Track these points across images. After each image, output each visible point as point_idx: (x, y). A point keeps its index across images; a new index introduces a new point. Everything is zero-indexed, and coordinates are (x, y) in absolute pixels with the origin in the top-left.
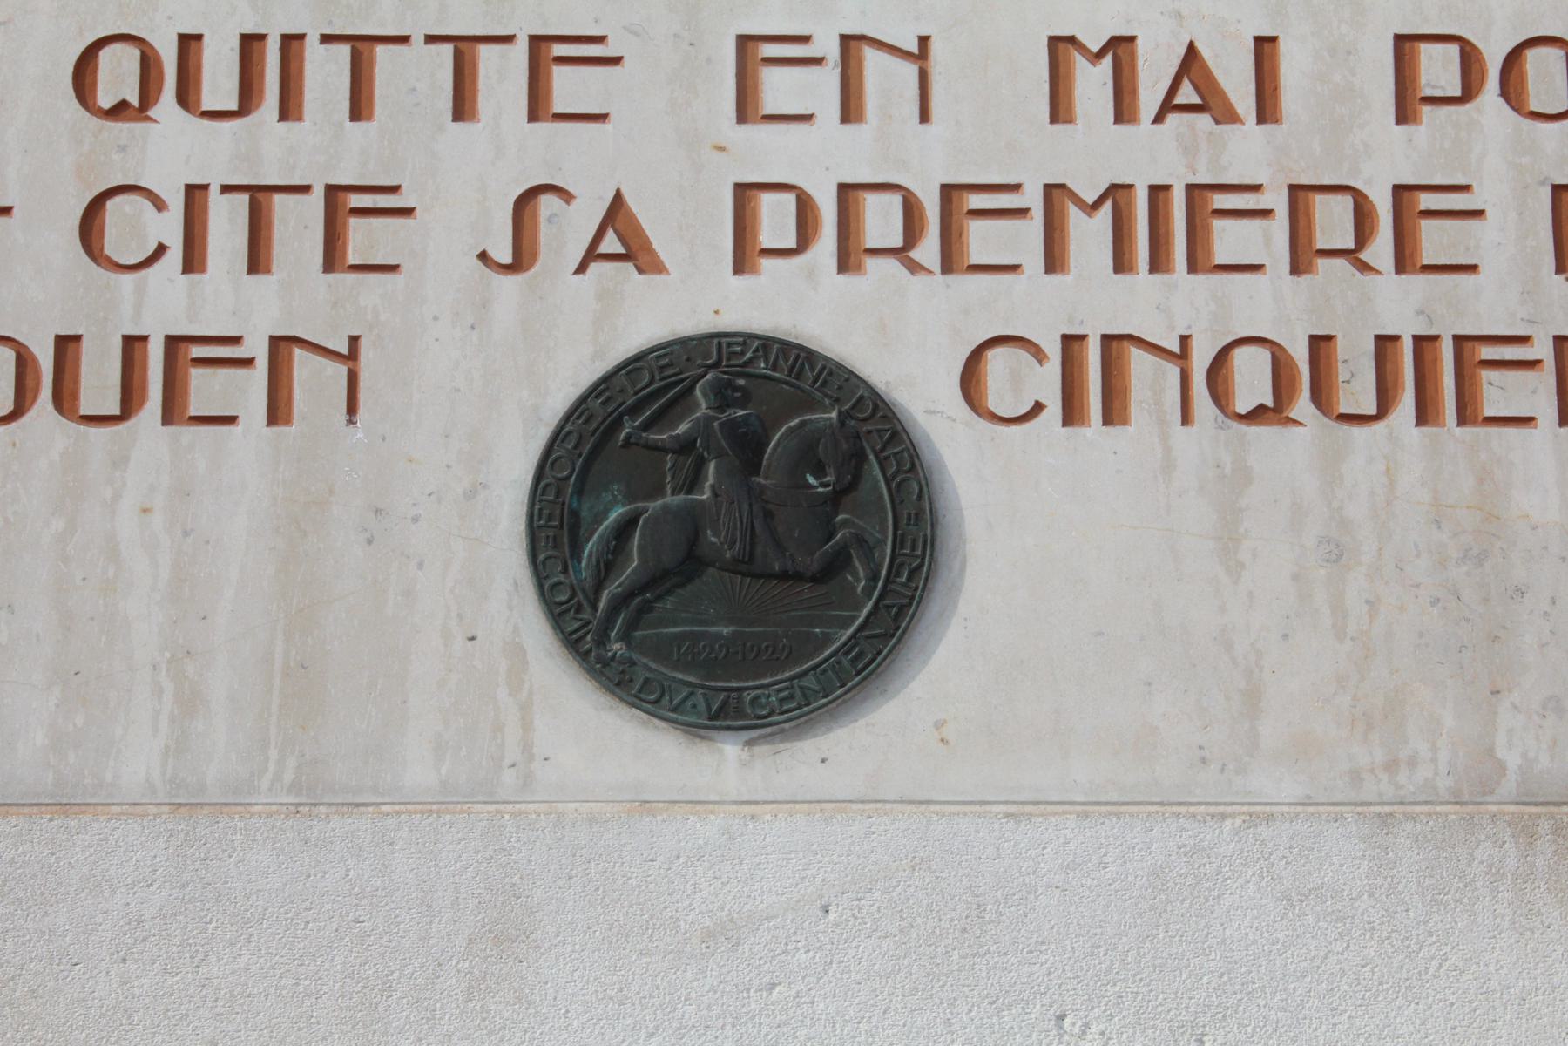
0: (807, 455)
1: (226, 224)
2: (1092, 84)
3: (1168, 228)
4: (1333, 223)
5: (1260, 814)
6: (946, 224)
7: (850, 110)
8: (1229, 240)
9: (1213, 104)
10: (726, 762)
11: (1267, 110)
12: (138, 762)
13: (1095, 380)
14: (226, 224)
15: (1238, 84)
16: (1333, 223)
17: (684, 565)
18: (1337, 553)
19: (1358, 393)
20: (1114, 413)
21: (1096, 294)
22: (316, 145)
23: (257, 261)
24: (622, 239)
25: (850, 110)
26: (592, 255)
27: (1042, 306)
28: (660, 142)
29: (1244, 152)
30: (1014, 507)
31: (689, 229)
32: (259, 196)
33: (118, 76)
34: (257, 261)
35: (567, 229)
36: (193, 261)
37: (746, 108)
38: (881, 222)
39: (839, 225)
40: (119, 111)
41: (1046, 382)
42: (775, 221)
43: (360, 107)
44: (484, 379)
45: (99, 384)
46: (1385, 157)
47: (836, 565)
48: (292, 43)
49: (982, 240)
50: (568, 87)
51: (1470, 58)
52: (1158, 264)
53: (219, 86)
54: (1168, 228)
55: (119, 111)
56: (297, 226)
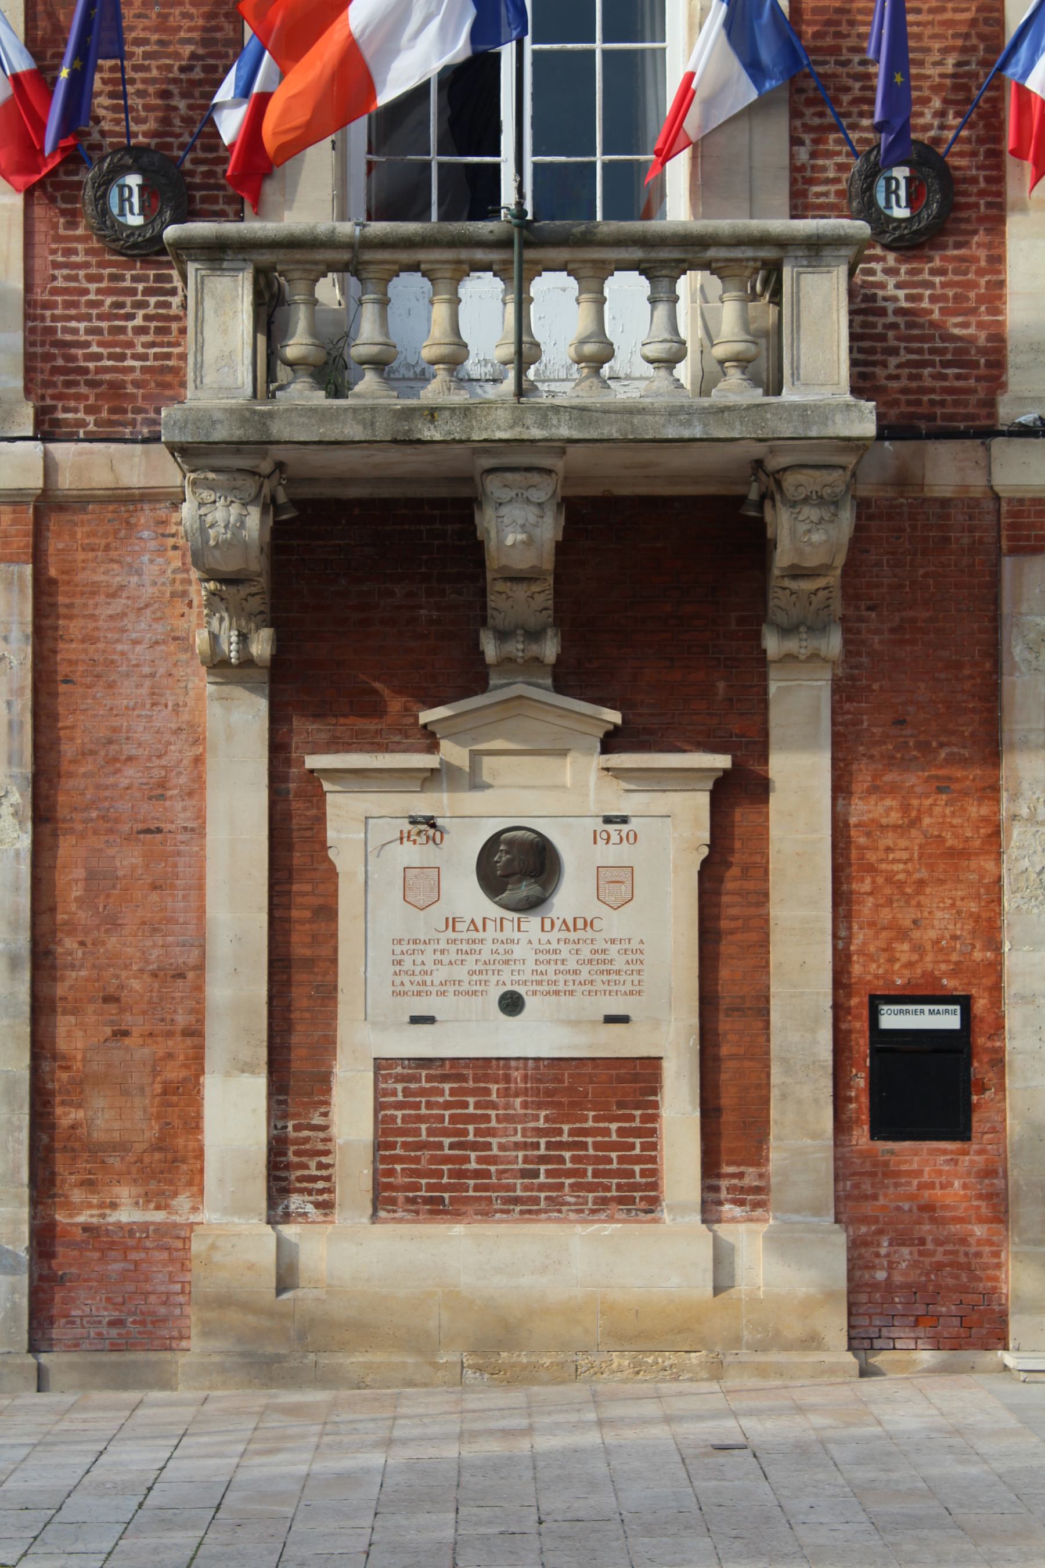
3: (540, 983)
6: (525, 982)
13: (534, 993)
21: (535, 987)
22: (483, 977)
24: (504, 984)
27: (531, 988)
28: (506, 976)
29: (545, 978)
30: (529, 1001)
31: (508, 983)
46: (554, 978)
54: (540, 983)
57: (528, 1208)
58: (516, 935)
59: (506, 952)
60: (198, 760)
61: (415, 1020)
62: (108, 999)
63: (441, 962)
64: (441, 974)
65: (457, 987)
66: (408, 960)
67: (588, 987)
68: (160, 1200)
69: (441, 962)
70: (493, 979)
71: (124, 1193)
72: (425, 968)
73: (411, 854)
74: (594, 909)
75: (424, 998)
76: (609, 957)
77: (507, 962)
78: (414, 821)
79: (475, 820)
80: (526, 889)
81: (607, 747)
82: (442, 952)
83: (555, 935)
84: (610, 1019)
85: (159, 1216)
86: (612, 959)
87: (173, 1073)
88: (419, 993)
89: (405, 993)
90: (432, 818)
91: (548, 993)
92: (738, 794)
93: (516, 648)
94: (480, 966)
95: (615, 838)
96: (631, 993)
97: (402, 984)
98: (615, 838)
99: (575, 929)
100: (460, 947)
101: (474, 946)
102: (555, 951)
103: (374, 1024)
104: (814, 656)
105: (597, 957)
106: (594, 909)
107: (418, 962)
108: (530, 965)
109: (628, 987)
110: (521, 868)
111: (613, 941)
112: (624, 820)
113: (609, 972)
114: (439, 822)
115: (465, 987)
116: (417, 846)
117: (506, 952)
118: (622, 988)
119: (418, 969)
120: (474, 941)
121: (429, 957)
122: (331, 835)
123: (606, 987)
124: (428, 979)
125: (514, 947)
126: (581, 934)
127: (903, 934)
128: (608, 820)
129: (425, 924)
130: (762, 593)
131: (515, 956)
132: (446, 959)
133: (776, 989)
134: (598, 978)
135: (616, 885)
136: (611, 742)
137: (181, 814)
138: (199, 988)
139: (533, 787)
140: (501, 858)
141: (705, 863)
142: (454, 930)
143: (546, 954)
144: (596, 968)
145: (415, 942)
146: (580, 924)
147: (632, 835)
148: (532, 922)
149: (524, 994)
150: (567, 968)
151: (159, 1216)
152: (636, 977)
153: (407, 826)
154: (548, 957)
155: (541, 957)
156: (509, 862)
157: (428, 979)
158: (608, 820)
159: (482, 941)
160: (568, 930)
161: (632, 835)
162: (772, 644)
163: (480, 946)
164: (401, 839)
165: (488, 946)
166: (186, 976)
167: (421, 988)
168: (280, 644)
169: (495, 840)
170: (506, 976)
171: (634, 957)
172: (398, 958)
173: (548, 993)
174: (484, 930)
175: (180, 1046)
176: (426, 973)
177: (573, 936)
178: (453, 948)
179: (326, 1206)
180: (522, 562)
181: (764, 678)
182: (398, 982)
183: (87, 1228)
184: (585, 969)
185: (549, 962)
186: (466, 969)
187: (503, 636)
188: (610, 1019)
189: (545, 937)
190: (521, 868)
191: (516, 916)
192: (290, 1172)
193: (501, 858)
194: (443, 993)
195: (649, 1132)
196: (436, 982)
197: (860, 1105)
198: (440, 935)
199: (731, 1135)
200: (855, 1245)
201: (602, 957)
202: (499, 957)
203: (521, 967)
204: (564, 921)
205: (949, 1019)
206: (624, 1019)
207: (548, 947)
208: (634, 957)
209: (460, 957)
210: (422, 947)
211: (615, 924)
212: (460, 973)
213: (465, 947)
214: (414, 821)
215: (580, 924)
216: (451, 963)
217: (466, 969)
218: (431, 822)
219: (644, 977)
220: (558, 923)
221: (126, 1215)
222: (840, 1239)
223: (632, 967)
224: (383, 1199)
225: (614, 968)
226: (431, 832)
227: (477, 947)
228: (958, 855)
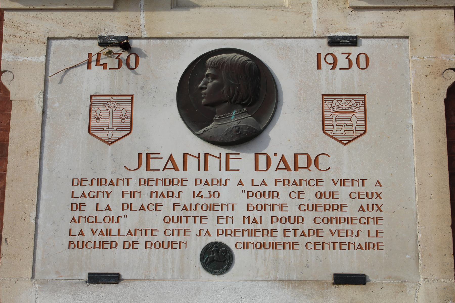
0: (222, 252)
1: (176, 232)
2: (246, 220)
3: (252, 233)
4: (266, 232)
5: (258, 281)
7: (227, 223)
8: (257, 234)
9: (256, 222)
10: (216, 277)
11: (261, 223)
12: (169, 276)
13: (246, 245)
14: (176, 232)
15: (258, 220)
16: (266, 232)
17: (212, 261)
18: (265, 260)
19: (267, 246)
20: (247, 248)
21: (246, 238)
22: (183, 226)
23: (178, 235)
24: (208, 233)
25: (227, 223)
26: (205, 235)
27: (242, 239)
28: (211, 225)
29: (259, 226)
30: (239, 255)
31: (213, 233)
32: (178, 230)
33: (167, 219)
34: (178, 235)
35: (203, 232)
36: (173, 235)
37: (218, 222)
38: (229, 232)
39: (225, 232)
40: (167, 223)
41: (242, 246)
42: (220, 232)
43: (187, 222)
44: (196, 245)
45: (166, 246)
46: (270, 227)
47: (225, 261)
48: (181, 217)
49: (237, 234)
50: (204, 221)
51: (277, 218)
52: (251, 236)
53: (175, 220)
54: (252, 233)
55: (167, 223)
56: (182, 232)
58: (224, 175)
59: (211, 195)
61: (95, 278)
63: (130, 207)
64: (131, 221)
65: (149, 238)
66: (90, 203)
67: (313, 239)
69: (130, 207)
70: (195, 228)
72: (111, 214)
73: (99, 80)
74: (320, 144)
75: (108, 252)
76: (339, 202)
77: (211, 207)
78: (104, 42)
80: (235, 120)
82: (133, 194)
83: (271, 175)
84: (341, 279)
88: (102, 245)
89: (85, 245)
90: (127, 38)
91: (263, 245)
94: (179, 212)
95: (342, 62)
96: (368, 246)
97: (81, 233)
98: (342, 62)
99: (296, 168)
100: (154, 188)
101: (171, 188)
102: (271, 195)
103: (43, 283)
105: (323, 201)
106: (320, 144)
107: (103, 206)
108: (241, 211)
109: (363, 239)
111: (343, 182)
112: (353, 41)
113: (338, 220)
114: (135, 44)
115: (160, 237)
116: (107, 71)
117: (211, 195)
118: (357, 241)
119: (101, 215)
120: (172, 182)
121: (116, 201)
123: (335, 239)
124: (114, 227)
125: (221, 189)
126: (303, 174)
128: (334, 42)
129: (113, 161)
131: (222, 200)
132: (136, 203)
134: (326, 228)
135: (345, 116)
139: (246, 7)
140: (207, 84)
142: (148, 168)
143: (261, 198)
144: (322, 215)
145: (99, 182)
146: (302, 161)
147: (362, 59)
148: (244, 160)
149: (232, 246)
150: (287, 215)
152: (373, 227)
153: (95, 47)
154: (263, 201)
155: (254, 201)
156: (216, 88)
157: (114, 227)
158: (334, 42)
159: (181, 182)
160: (287, 168)
161: (362, 59)
163: (179, 188)
164: (89, 63)
165: (190, 187)
167: (105, 239)
169: (199, 64)
170: (211, 225)
171: (370, 202)
172: (78, 201)
173: (263, 245)
174: (185, 168)
176: (111, 220)
177: (293, 176)
178: (146, 190)
182: (76, 231)
184: (309, 216)
185: (264, 207)
186: (161, 215)
188: (341, 279)
189: (259, 177)
191: (224, 151)
193: (207, 84)
194: (132, 245)
196: (124, 232)
198: (132, 175)
201: (330, 201)
202: (202, 201)
203: (230, 213)
204: (283, 158)
206: (359, 279)
207: (262, 189)
208: (370, 202)
209: (154, 201)
210: (108, 188)
211: (345, 161)
212: (154, 220)
213: (161, 188)
214: (104, 42)
215: (302, 161)
216: (142, 208)
217: (161, 215)
218: (124, 43)
219: (384, 226)
220: (275, 161)
223: (367, 214)
225: (346, 215)
226: (124, 55)
227: (176, 189)
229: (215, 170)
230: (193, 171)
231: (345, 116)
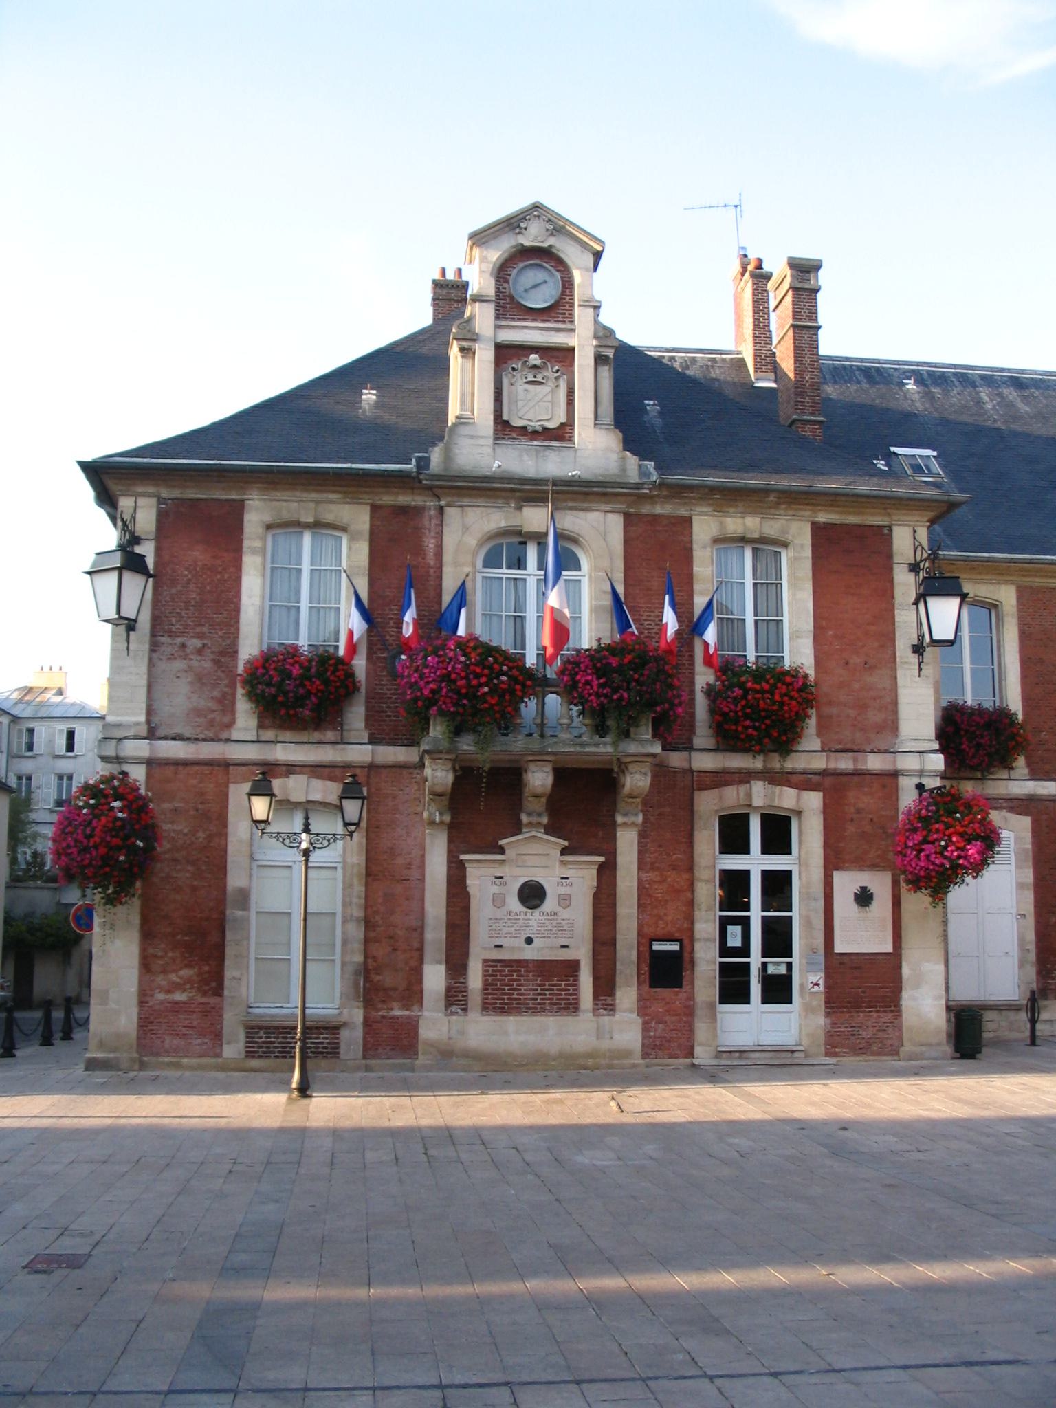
30: (535, 941)
57: (534, 1011)
60: (423, 856)
62: (391, 938)
64: (506, 930)
68: (407, 1007)
71: (395, 1004)
73: (495, 889)
79: (517, 877)
80: (537, 902)
81: (562, 854)
85: (407, 1013)
86: (563, 928)
87: (413, 963)
92: (607, 871)
93: (535, 819)
104: (634, 824)
110: (532, 895)
122: (468, 882)
127: (660, 918)
129: (500, 913)
130: (614, 803)
133: (619, 937)
136: (564, 852)
137: (415, 874)
138: (422, 934)
141: (595, 894)
148: (536, 912)
151: (407, 1013)
162: (620, 819)
166: (419, 930)
168: (452, 818)
175: (416, 954)
179: (465, 1010)
180: (539, 791)
181: (615, 830)
183: (383, 1017)
187: (529, 814)
190: (532, 895)
192: (455, 997)
195: (576, 985)
197: (646, 977)
199: (605, 988)
200: (645, 1023)
205: (675, 947)
211: (565, 914)
212: (512, 930)
221: (397, 1012)
222: (639, 1020)
224: (486, 1007)
228: (678, 891)
229: (529, 916)
230: (523, 916)
231: (565, 900)
